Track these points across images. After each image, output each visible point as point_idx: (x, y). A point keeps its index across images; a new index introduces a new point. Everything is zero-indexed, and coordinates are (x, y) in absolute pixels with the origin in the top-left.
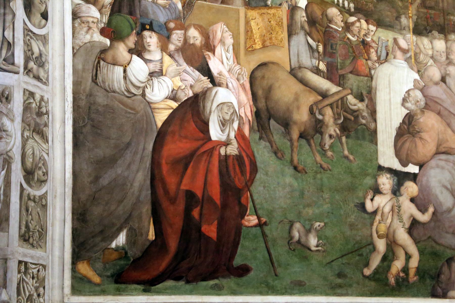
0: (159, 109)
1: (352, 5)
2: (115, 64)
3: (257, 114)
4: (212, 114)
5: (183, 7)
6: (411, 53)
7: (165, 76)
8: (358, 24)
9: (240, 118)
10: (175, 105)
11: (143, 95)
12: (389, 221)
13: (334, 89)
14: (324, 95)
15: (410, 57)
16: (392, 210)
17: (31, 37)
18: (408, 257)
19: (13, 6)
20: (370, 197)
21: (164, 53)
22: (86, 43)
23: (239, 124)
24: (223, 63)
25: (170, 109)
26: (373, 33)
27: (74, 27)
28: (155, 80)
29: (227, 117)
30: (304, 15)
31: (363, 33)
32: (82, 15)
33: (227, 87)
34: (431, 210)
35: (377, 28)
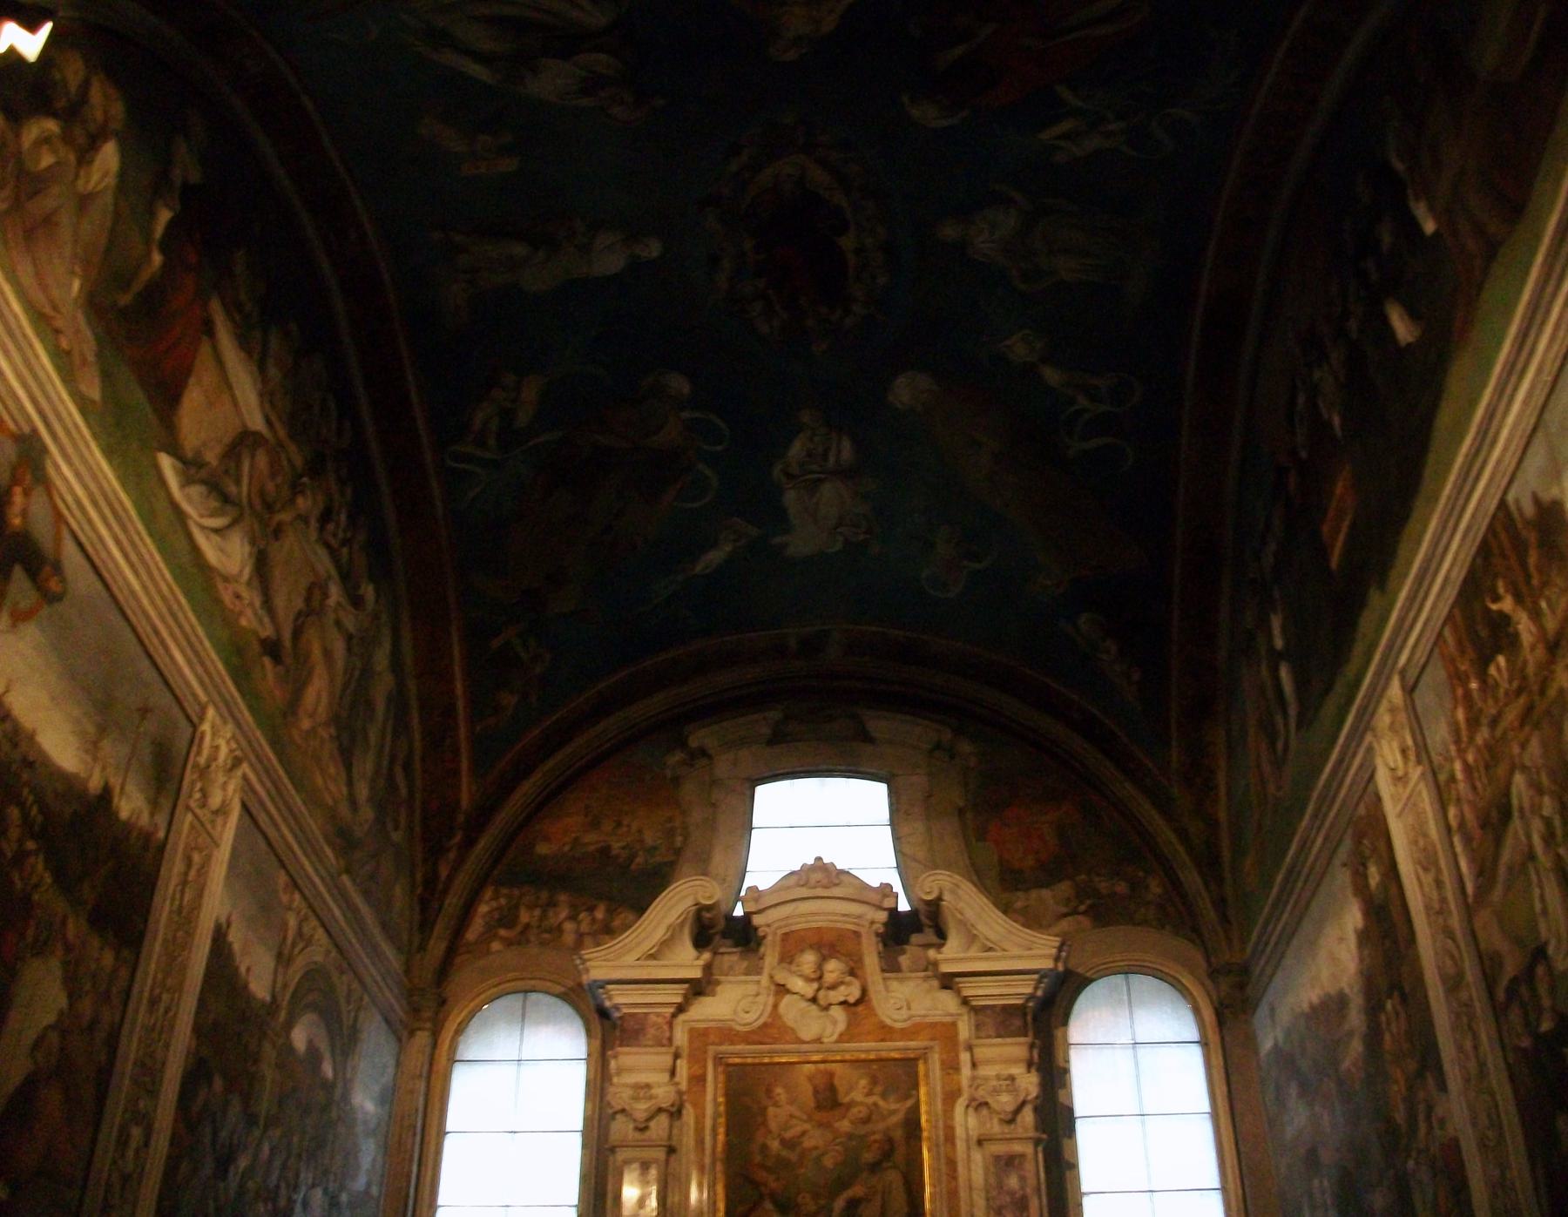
8: (32, 860)
15: (70, 962)
26: (45, 887)
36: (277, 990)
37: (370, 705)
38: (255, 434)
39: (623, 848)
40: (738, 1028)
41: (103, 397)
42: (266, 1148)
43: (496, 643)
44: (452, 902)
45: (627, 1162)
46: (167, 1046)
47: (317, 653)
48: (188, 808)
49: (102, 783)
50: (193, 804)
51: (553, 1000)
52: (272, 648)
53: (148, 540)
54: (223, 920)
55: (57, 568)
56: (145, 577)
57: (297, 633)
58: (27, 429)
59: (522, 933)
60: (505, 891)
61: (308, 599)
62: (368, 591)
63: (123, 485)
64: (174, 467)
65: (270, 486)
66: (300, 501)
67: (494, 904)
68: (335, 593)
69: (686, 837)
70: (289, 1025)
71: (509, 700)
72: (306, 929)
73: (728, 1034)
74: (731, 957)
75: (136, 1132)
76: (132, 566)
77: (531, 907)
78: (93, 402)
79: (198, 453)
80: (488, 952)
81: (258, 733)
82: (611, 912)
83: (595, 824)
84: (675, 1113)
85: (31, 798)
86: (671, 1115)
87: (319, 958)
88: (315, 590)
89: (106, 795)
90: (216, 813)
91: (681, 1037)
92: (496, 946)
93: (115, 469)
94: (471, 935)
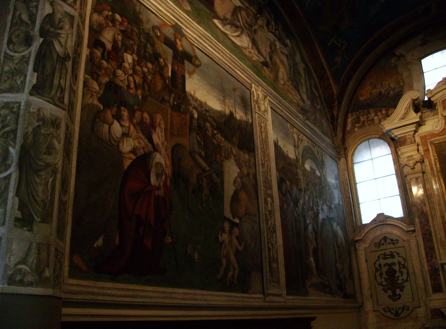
0: (126, 157)
1: (215, 124)
2: (105, 122)
3: (174, 174)
4: (152, 168)
5: (142, 98)
6: (237, 158)
7: (131, 137)
8: (217, 135)
9: (166, 174)
10: (134, 157)
11: (118, 147)
12: (228, 248)
13: (208, 168)
14: (204, 170)
16: (229, 242)
18: (234, 270)
20: (220, 233)
21: (131, 124)
22: (89, 104)
23: (165, 178)
24: (159, 138)
25: (131, 159)
26: (223, 142)
27: (83, 91)
28: (125, 139)
29: (160, 172)
30: (196, 122)
31: (219, 141)
32: (89, 85)
33: (160, 153)
34: (243, 244)
35: (225, 140)
36: (297, 155)
37: (299, 73)
38: (239, 7)
39: (385, 91)
40: (436, 132)
41: (191, 9)
42: (307, 197)
43: (329, 44)
44: (340, 121)
45: (411, 179)
46: (271, 176)
47: (278, 62)
48: (256, 112)
49: (229, 111)
50: (257, 111)
51: (377, 140)
52: (265, 64)
53: (219, 44)
54: (276, 140)
55: (196, 57)
56: (221, 53)
57: (271, 59)
58: (174, 24)
59: (363, 123)
60: (354, 113)
61: (271, 48)
62: (288, 42)
63: (206, 31)
64: (219, 22)
65: (249, 20)
66: (259, 22)
67: (352, 118)
68: (278, 44)
69: (404, 82)
70: (303, 164)
71: (338, 59)
72: (300, 137)
73: (432, 135)
74: (427, 113)
75: (269, 199)
76: (217, 52)
77: (363, 116)
78: (189, 11)
79: (224, 17)
80: (354, 131)
81: (269, 88)
82: (387, 110)
83: (375, 87)
84: (422, 162)
85: (211, 120)
86: (421, 162)
87: (307, 144)
88: (272, 46)
89: (231, 114)
90: (264, 112)
91: (418, 140)
92: (356, 129)
93: (202, 27)
94: (348, 128)
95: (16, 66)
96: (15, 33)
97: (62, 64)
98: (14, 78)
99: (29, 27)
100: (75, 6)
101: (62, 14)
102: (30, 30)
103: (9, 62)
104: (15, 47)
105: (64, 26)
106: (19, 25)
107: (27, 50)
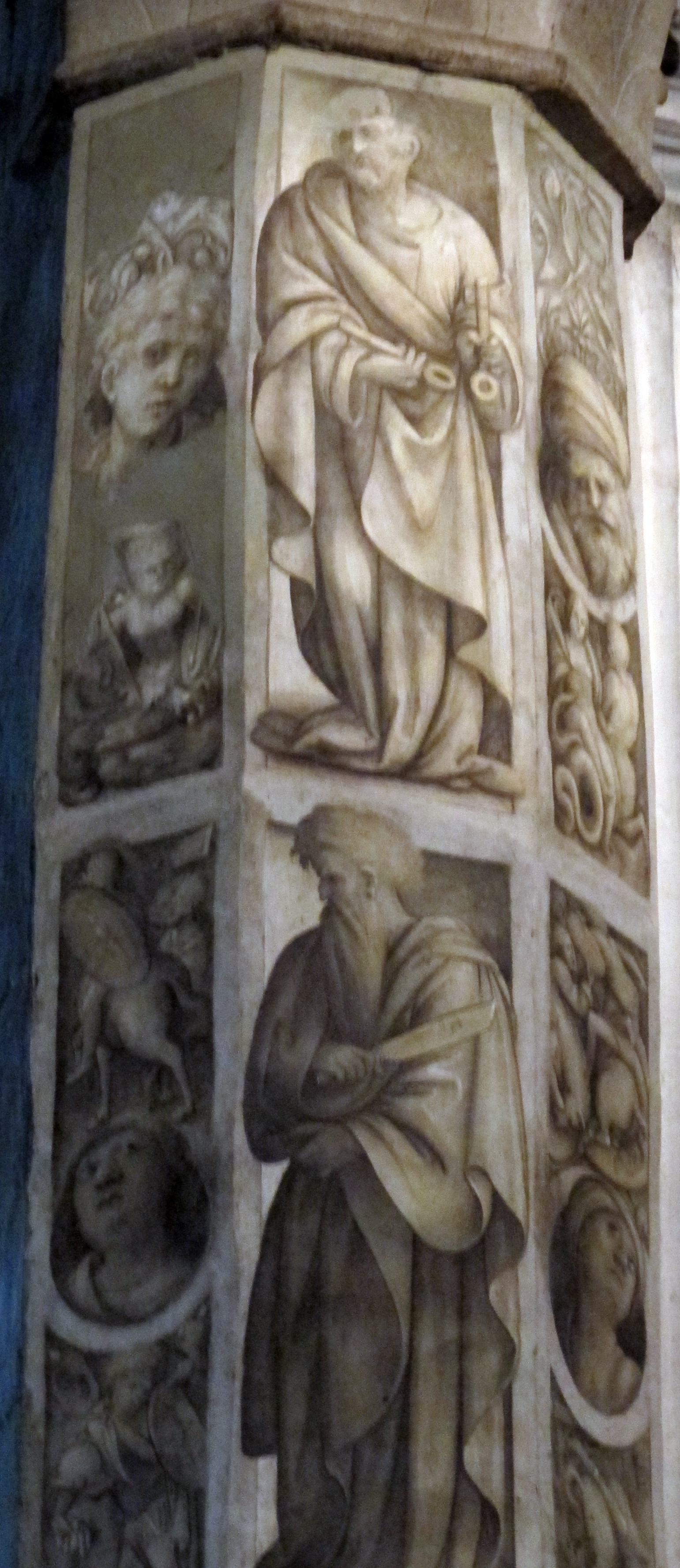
17: (582, 1470)
19: (501, 1294)
95: (128, 1435)
96: (93, 1169)
97: (462, 1314)
98: (130, 1529)
99: (176, 1099)
100: (503, 776)
101: (401, 897)
102: (186, 1118)
103: (81, 1407)
104: (104, 1277)
105: (434, 986)
106: (111, 1102)
107: (179, 1287)
